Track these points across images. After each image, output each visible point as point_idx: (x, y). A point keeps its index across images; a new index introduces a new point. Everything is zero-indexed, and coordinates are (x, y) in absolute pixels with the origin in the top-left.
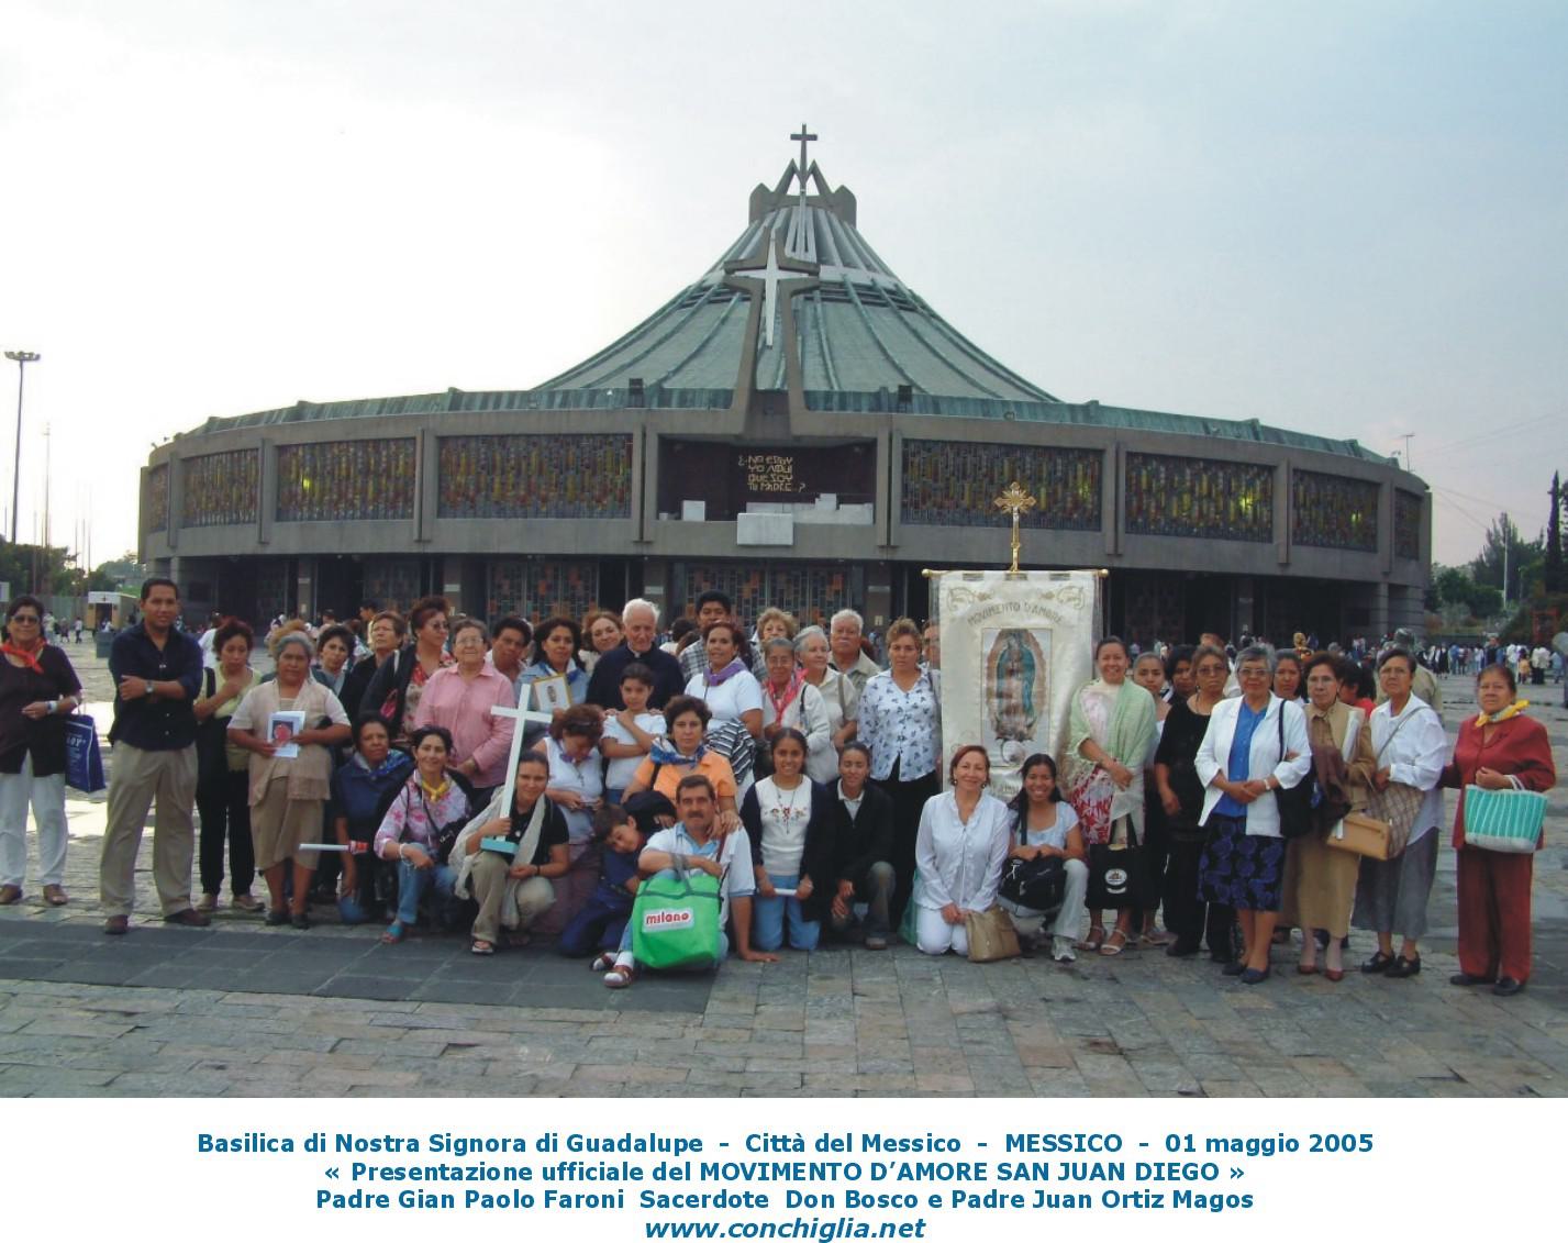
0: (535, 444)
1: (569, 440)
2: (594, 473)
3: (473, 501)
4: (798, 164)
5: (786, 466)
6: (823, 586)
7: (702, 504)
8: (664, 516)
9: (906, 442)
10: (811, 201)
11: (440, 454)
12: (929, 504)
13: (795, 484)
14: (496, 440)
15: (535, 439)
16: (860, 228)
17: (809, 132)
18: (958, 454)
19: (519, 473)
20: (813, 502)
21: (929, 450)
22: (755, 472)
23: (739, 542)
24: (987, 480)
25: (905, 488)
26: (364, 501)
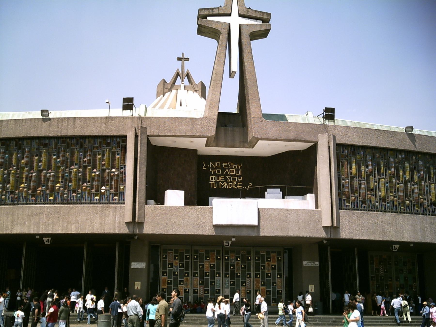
0: (46, 145)
1: (75, 141)
5: (238, 170)
6: (263, 262)
7: (181, 194)
13: (244, 183)
14: (14, 143)
15: (47, 142)
17: (185, 57)
22: (215, 174)
23: (216, 222)
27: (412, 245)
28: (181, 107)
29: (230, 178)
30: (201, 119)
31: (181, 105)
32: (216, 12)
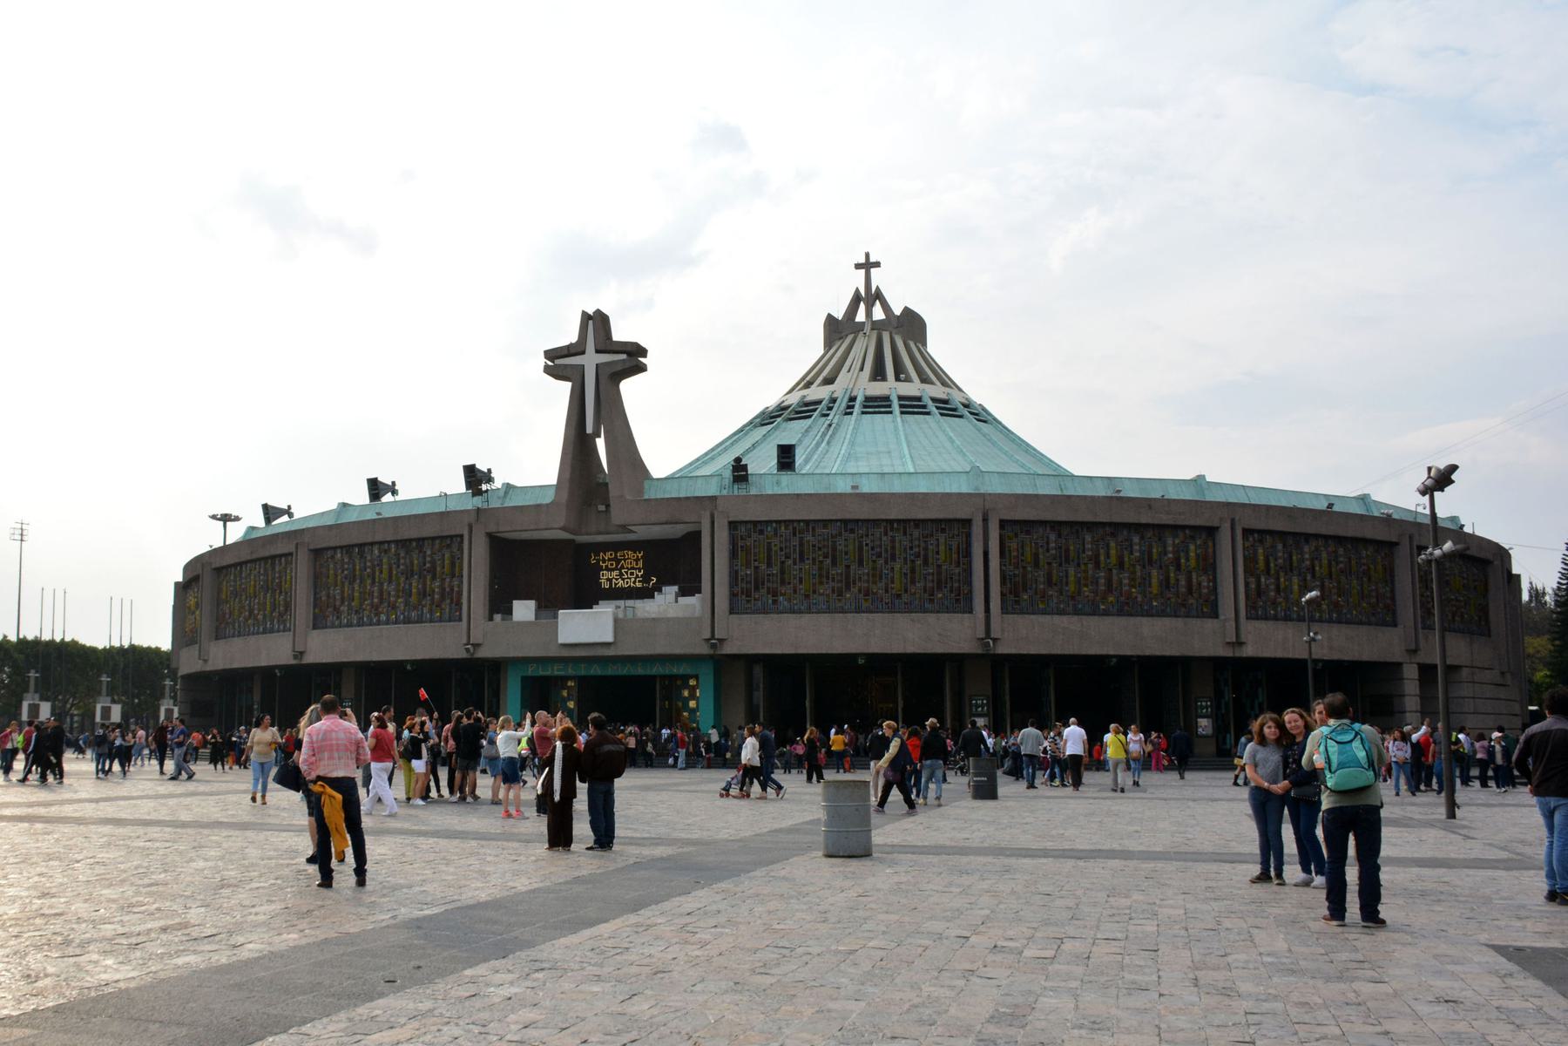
2: (434, 578)
5: (637, 560)
7: (532, 604)
8: (498, 617)
9: (733, 525)
10: (877, 326)
11: (315, 568)
12: (763, 591)
13: (646, 579)
16: (928, 350)
17: (872, 259)
18: (794, 534)
19: (374, 579)
20: (653, 597)
21: (761, 532)
22: (607, 569)
23: (561, 641)
24: (829, 561)
25: (734, 577)
26: (265, 616)
27: (861, 661)
29: (627, 573)
30: (547, 505)
31: (849, 371)
32: (566, 352)
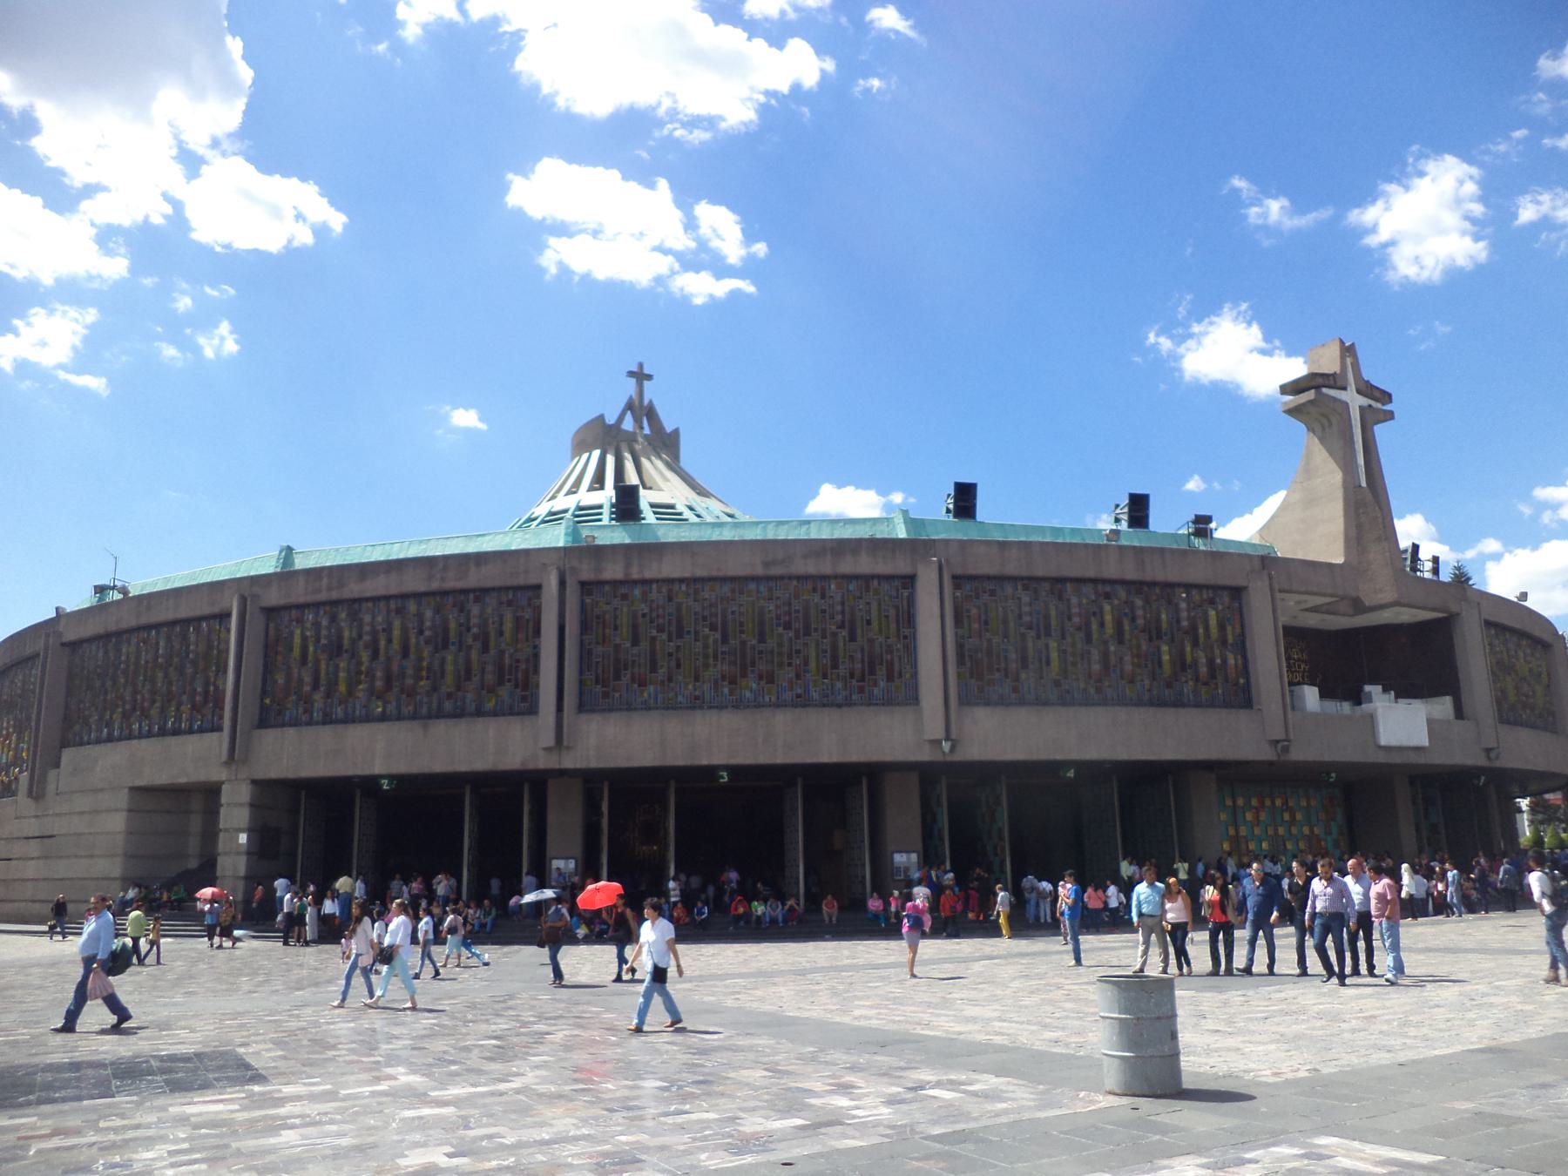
3: (1017, 679)
4: (637, 403)
17: (646, 371)
28: (1436, 555)
